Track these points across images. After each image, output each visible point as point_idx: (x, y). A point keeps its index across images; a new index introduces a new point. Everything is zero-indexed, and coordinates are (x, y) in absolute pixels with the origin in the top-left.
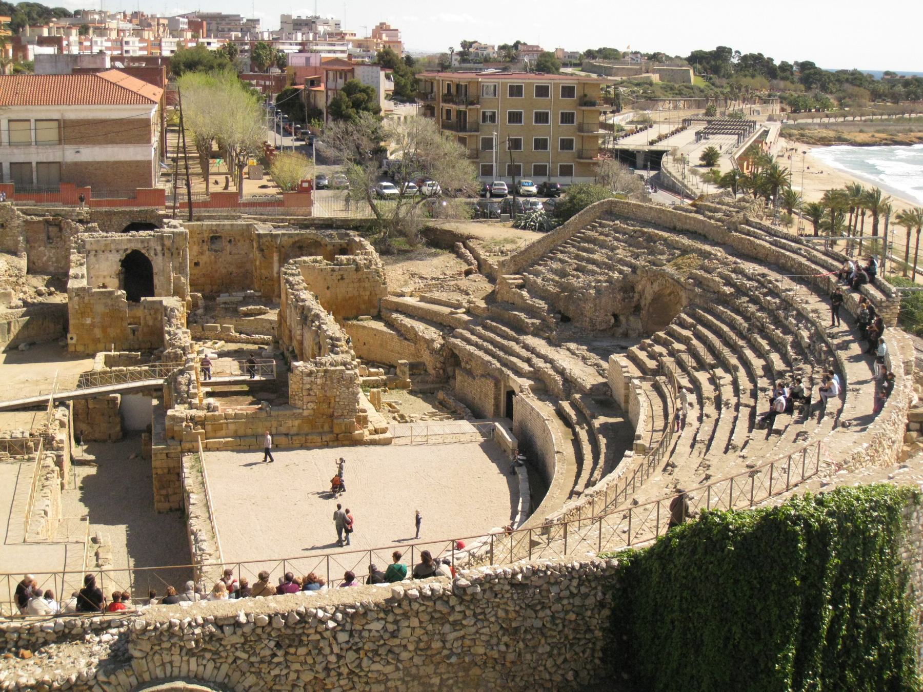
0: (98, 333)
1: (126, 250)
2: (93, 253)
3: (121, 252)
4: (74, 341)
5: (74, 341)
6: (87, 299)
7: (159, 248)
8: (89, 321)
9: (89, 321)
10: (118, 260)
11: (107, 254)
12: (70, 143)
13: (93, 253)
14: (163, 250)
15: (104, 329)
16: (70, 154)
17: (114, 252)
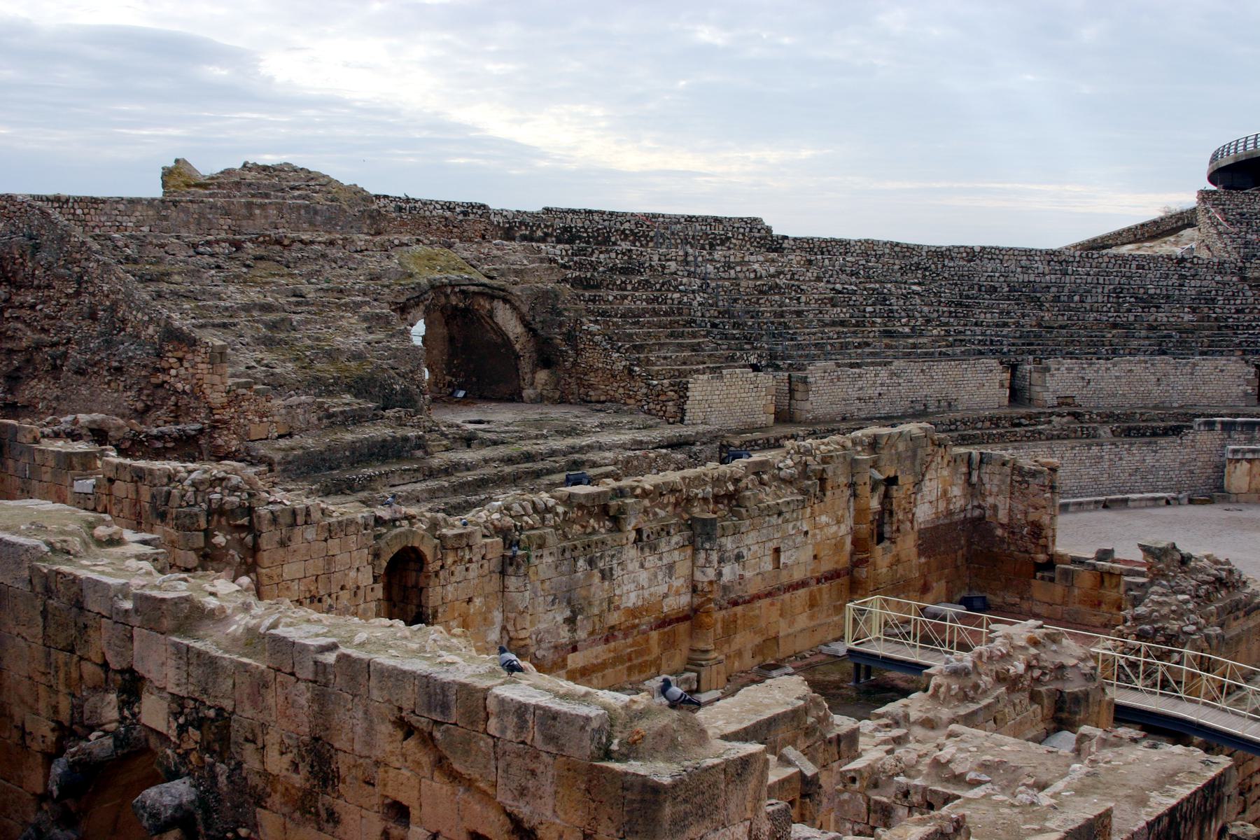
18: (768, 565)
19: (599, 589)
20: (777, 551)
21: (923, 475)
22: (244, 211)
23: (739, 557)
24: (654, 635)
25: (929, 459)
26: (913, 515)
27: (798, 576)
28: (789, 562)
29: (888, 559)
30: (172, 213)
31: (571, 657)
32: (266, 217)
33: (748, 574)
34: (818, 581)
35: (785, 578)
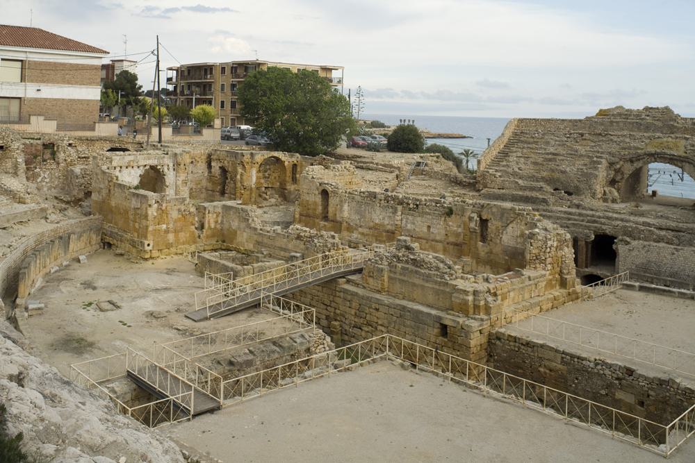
0: (171, 237)
1: (145, 166)
2: (118, 169)
3: (141, 168)
4: (150, 248)
5: (150, 248)
6: (164, 205)
7: (171, 165)
8: (164, 226)
9: (164, 226)
10: (138, 175)
11: (130, 168)
12: (32, 81)
13: (118, 169)
14: (174, 165)
15: (176, 232)
16: (30, 91)
17: (135, 168)
18: (425, 229)
19: (367, 215)
20: (429, 227)
21: (508, 225)
22: (609, 124)
23: (414, 224)
24: (384, 234)
25: (512, 219)
26: (501, 238)
27: (438, 238)
28: (435, 232)
29: (486, 250)
30: (579, 124)
31: (360, 229)
32: (618, 126)
33: (417, 229)
34: (448, 244)
35: (432, 237)
